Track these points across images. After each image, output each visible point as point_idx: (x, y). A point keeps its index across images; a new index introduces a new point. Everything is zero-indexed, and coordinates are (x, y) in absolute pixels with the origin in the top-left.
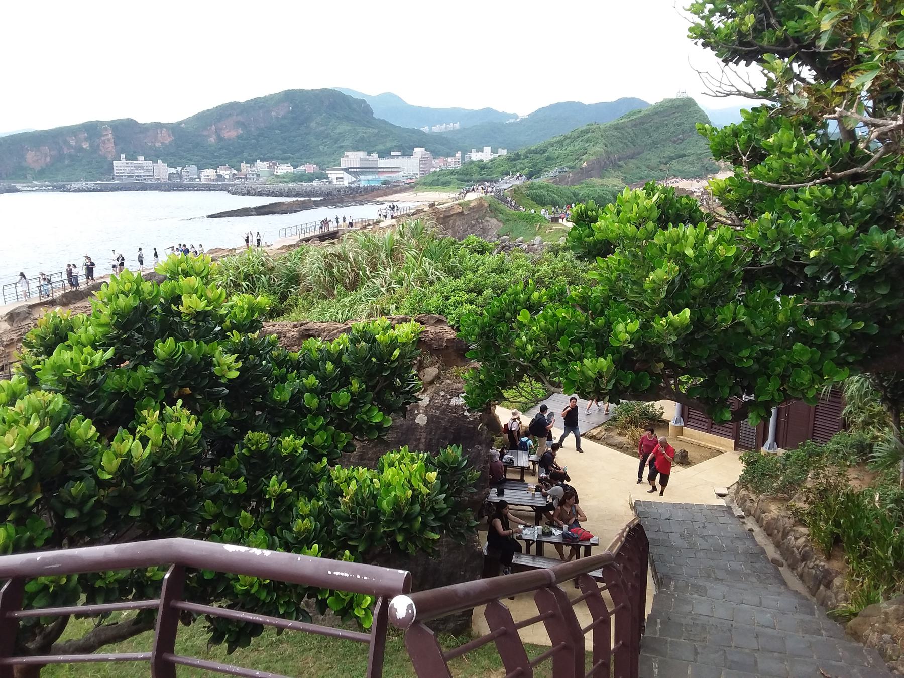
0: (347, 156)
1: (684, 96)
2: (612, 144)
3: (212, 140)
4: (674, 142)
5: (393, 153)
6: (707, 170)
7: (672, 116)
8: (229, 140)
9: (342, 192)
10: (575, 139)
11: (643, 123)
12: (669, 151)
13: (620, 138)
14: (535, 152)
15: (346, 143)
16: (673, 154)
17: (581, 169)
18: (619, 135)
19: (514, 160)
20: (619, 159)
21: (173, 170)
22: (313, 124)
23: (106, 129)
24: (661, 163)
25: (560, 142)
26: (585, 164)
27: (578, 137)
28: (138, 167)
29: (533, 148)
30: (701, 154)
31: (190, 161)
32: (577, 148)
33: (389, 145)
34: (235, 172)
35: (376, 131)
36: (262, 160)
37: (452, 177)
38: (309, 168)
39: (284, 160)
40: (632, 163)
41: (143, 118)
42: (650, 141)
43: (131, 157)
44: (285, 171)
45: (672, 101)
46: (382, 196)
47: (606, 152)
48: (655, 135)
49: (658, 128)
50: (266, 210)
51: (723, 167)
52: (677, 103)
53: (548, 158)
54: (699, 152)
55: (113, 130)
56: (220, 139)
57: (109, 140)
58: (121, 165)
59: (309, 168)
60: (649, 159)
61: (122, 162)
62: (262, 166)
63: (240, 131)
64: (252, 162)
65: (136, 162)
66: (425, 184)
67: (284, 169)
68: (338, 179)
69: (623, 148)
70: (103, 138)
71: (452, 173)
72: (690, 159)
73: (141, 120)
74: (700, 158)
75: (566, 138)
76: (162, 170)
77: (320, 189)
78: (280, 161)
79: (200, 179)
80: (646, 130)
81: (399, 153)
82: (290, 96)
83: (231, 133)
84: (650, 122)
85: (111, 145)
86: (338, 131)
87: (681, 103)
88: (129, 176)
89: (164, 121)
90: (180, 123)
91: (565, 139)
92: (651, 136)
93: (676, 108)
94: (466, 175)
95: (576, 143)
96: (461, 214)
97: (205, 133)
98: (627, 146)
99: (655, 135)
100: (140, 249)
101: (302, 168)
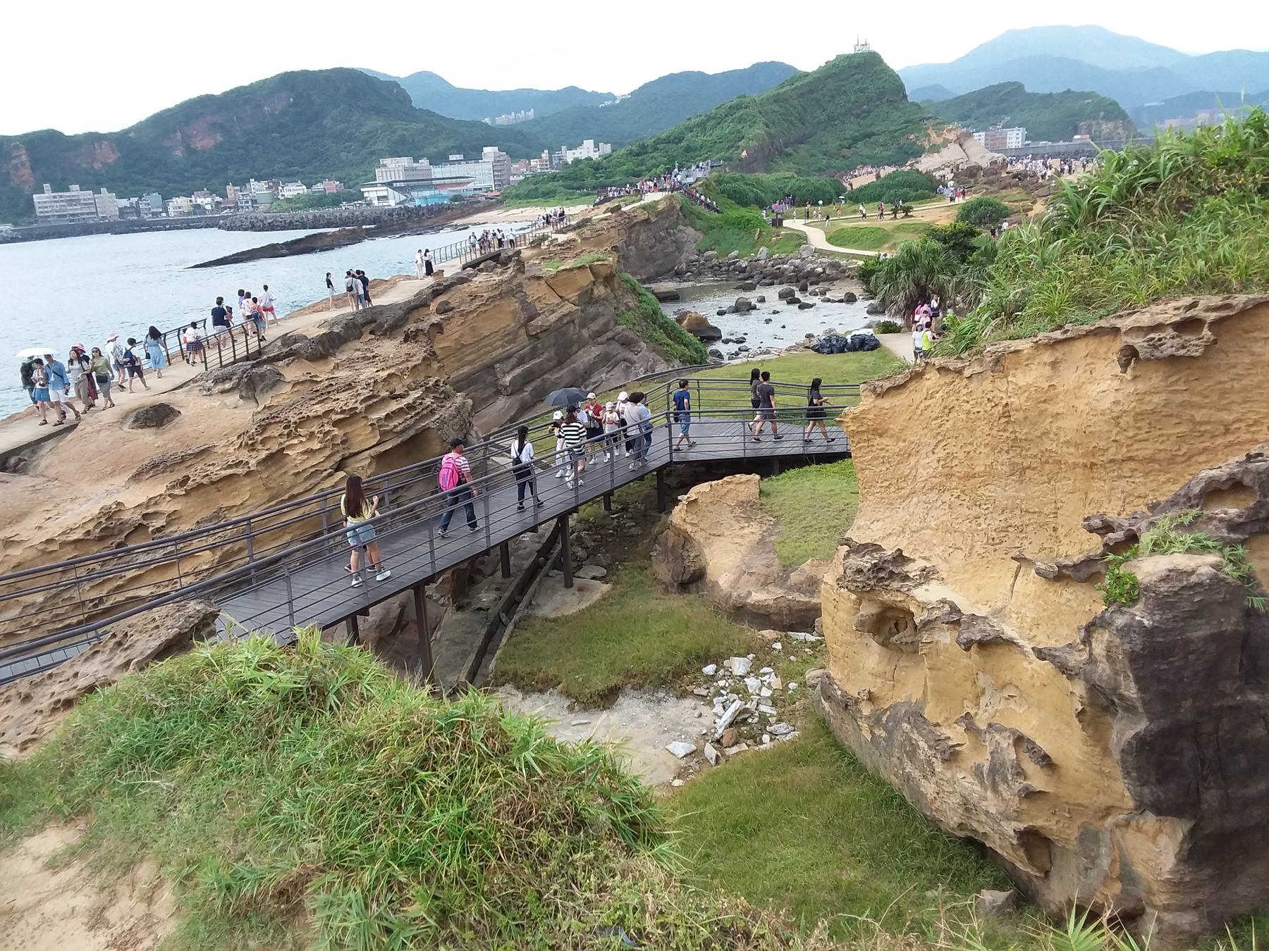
0: (385, 166)
1: (865, 49)
2: (773, 123)
3: (179, 153)
4: (857, 116)
5: (452, 158)
6: (906, 153)
8: (204, 152)
9: (395, 217)
10: (720, 120)
12: (852, 129)
14: (667, 141)
15: (379, 146)
17: (741, 160)
18: (782, 110)
19: (638, 155)
21: (124, 202)
22: (327, 122)
23: (17, 148)
24: (842, 147)
25: (702, 126)
26: (744, 154)
27: (726, 116)
28: (71, 202)
29: (663, 136)
30: (895, 131)
31: (149, 187)
32: (727, 132)
33: (442, 145)
34: (218, 199)
35: (422, 126)
36: (258, 179)
37: (555, 183)
38: (330, 186)
39: (290, 177)
40: (803, 150)
41: (71, 127)
42: (824, 117)
43: (60, 187)
44: (295, 193)
45: (849, 57)
46: (459, 218)
47: (769, 134)
49: (833, 97)
50: (302, 246)
51: (927, 147)
53: (688, 149)
54: (892, 128)
55: (27, 150)
56: (190, 151)
57: (23, 164)
58: (44, 200)
59: (330, 186)
61: (46, 195)
62: (258, 188)
63: (219, 138)
64: (242, 183)
65: (66, 194)
66: (518, 197)
67: (293, 190)
68: (379, 198)
70: (14, 162)
71: (554, 178)
73: (69, 131)
74: (894, 137)
75: (709, 118)
76: (109, 203)
77: (362, 213)
78: (284, 179)
79: (167, 212)
81: (460, 157)
82: (290, 82)
83: (205, 142)
85: (26, 172)
86: (364, 129)
88: (59, 216)
89: (103, 130)
90: (126, 132)
91: (708, 120)
92: (824, 110)
93: (856, 68)
94: (575, 179)
95: (725, 125)
96: (647, 221)
97: (167, 144)
100: (266, 288)
101: (320, 187)
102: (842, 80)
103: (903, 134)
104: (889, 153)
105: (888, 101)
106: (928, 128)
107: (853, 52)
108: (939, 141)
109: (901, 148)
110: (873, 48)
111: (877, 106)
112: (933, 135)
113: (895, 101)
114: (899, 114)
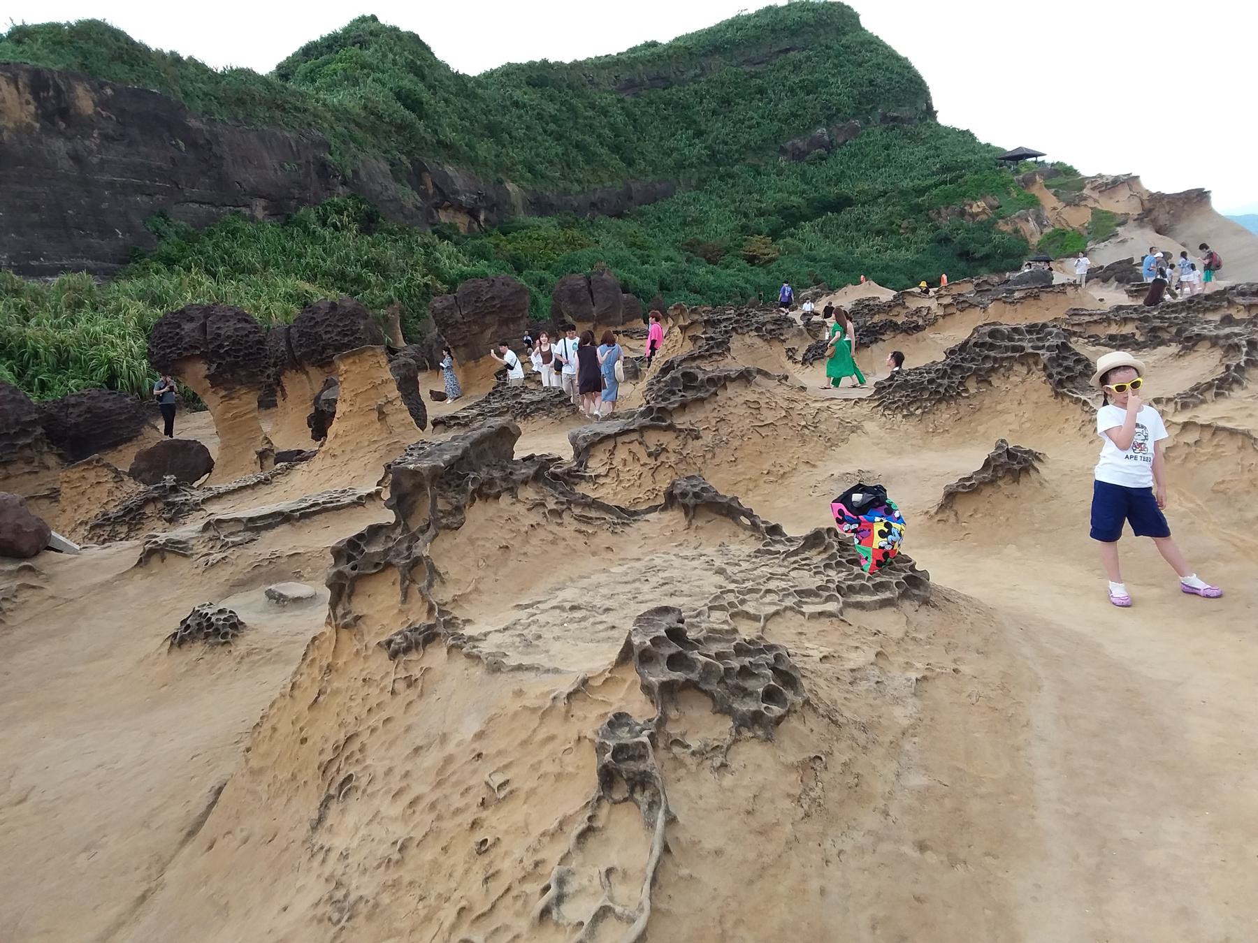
4: (799, 155)
6: (965, 255)
7: (778, 61)
11: (667, 82)
13: (554, 119)
16: (795, 200)
18: (551, 108)
20: (540, 206)
30: (920, 192)
42: (699, 149)
48: (719, 128)
49: (726, 102)
51: (1035, 240)
52: (796, 15)
54: (906, 184)
60: (697, 221)
72: (876, 216)
74: (917, 209)
84: (695, 79)
92: (699, 134)
98: (590, 158)
99: (719, 128)
102: (749, 62)
103: (948, 199)
104: (903, 255)
105: (884, 118)
106: (1028, 182)
108: (1078, 218)
109: (945, 240)
111: (854, 132)
112: (1049, 201)
113: (910, 121)
114: (921, 151)
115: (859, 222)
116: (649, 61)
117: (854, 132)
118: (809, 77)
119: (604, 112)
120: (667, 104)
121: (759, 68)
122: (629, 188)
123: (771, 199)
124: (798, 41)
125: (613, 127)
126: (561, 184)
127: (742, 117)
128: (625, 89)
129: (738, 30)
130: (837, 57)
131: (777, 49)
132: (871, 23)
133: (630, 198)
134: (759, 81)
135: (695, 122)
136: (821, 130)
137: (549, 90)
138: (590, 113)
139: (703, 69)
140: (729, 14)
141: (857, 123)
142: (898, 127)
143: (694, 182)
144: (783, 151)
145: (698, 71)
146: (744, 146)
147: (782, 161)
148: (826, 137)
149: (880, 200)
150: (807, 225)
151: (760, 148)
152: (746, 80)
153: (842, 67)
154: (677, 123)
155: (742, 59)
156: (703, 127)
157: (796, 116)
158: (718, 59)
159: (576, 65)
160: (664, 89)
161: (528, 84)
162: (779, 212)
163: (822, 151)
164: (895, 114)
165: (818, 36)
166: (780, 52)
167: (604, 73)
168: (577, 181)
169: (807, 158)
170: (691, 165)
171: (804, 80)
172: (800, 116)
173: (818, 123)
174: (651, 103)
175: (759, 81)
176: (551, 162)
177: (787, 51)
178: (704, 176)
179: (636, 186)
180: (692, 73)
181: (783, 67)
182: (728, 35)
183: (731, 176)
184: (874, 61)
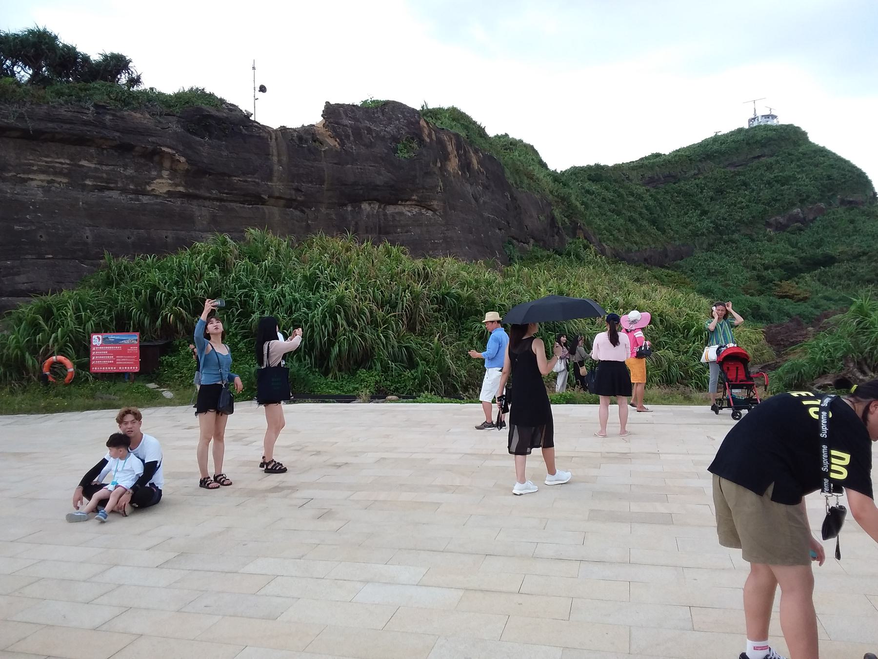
4: (780, 227)
7: (755, 163)
11: (675, 179)
16: (790, 258)
18: (609, 195)
45: (740, 130)
48: (719, 210)
49: (720, 191)
69: (628, 232)
80: (687, 194)
87: (771, 134)
92: (704, 213)
93: (763, 146)
99: (719, 210)
107: (746, 127)
110: (783, 119)
113: (863, 203)
115: (850, 275)
116: (662, 165)
117: (821, 211)
118: (781, 174)
119: (640, 198)
120: (679, 193)
121: (740, 169)
122: (665, 249)
123: (769, 258)
124: (766, 151)
125: (647, 207)
126: (627, 245)
127: (733, 202)
128: (648, 184)
129: (722, 144)
130: (799, 160)
131: (752, 156)
132: (817, 137)
133: (666, 256)
134: (742, 178)
135: (700, 205)
136: (796, 210)
137: (604, 183)
138: (632, 199)
139: (699, 170)
140: (709, 134)
141: (822, 205)
142: (856, 208)
143: (705, 246)
144: (768, 225)
145: (696, 172)
146: (739, 221)
147: (770, 232)
148: (801, 215)
149: (865, 258)
150: (807, 277)
151: (751, 223)
152: (732, 176)
153: (804, 167)
154: (688, 205)
155: (727, 163)
156: (706, 209)
157: (776, 200)
158: (710, 164)
159: (617, 168)
160: (674, 183)
161: (589, 180)
162: (781, 267)
163: (799, 224)
164: (851, 199)
165: (781, 147)
166: (755, 158)
167: (635, 173)
168: (635, 243)
169: (789, 229)
170: (703, 234)
171: (778, 176)
172: (779, 200)
173: (793, 205)
174: (667, 192)
175: (742, 178)
176: (619, 230)
177: (759, 157)
178: (712, 241)
179: (669, 248)
180: (692, 172)
181: (758, 168)
182: (715, 147)
183: (733, 241)
184: (828, 163)
